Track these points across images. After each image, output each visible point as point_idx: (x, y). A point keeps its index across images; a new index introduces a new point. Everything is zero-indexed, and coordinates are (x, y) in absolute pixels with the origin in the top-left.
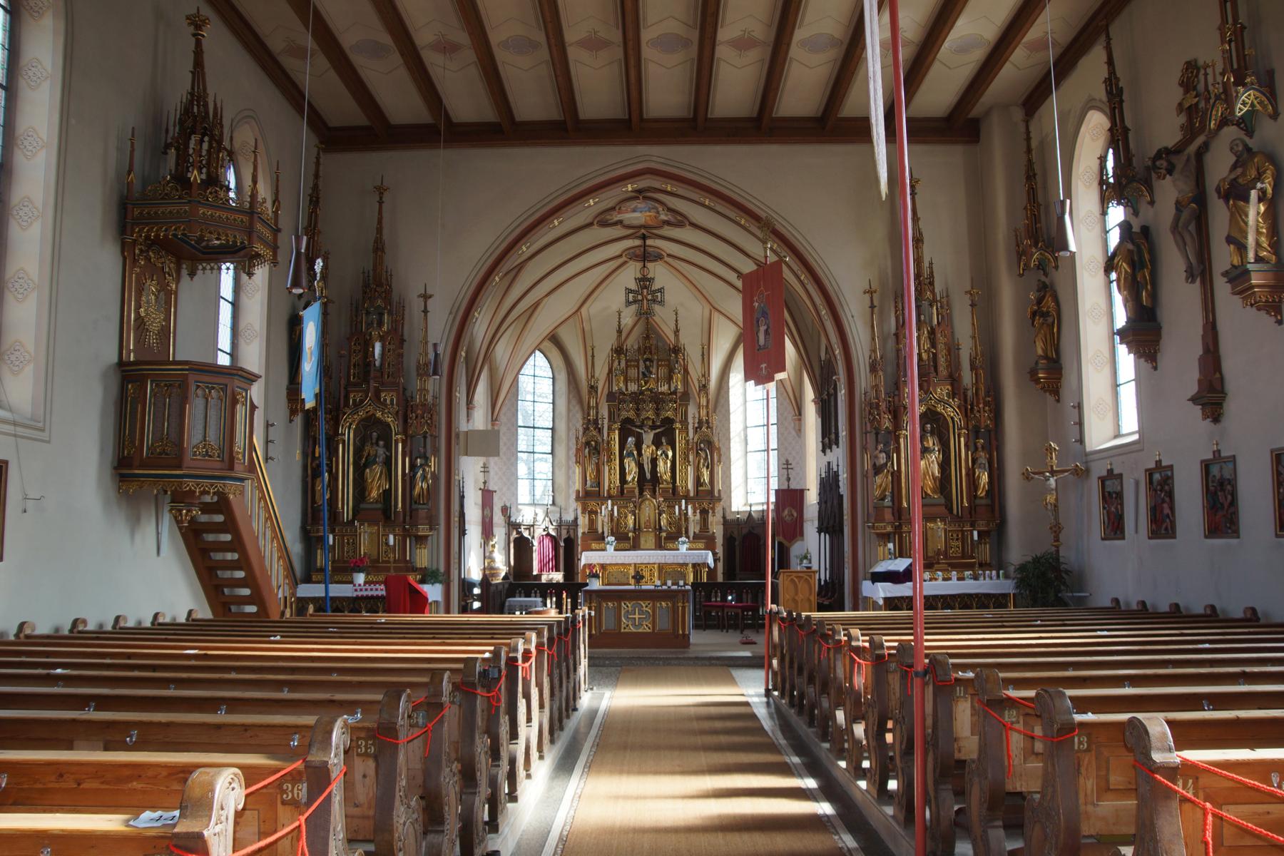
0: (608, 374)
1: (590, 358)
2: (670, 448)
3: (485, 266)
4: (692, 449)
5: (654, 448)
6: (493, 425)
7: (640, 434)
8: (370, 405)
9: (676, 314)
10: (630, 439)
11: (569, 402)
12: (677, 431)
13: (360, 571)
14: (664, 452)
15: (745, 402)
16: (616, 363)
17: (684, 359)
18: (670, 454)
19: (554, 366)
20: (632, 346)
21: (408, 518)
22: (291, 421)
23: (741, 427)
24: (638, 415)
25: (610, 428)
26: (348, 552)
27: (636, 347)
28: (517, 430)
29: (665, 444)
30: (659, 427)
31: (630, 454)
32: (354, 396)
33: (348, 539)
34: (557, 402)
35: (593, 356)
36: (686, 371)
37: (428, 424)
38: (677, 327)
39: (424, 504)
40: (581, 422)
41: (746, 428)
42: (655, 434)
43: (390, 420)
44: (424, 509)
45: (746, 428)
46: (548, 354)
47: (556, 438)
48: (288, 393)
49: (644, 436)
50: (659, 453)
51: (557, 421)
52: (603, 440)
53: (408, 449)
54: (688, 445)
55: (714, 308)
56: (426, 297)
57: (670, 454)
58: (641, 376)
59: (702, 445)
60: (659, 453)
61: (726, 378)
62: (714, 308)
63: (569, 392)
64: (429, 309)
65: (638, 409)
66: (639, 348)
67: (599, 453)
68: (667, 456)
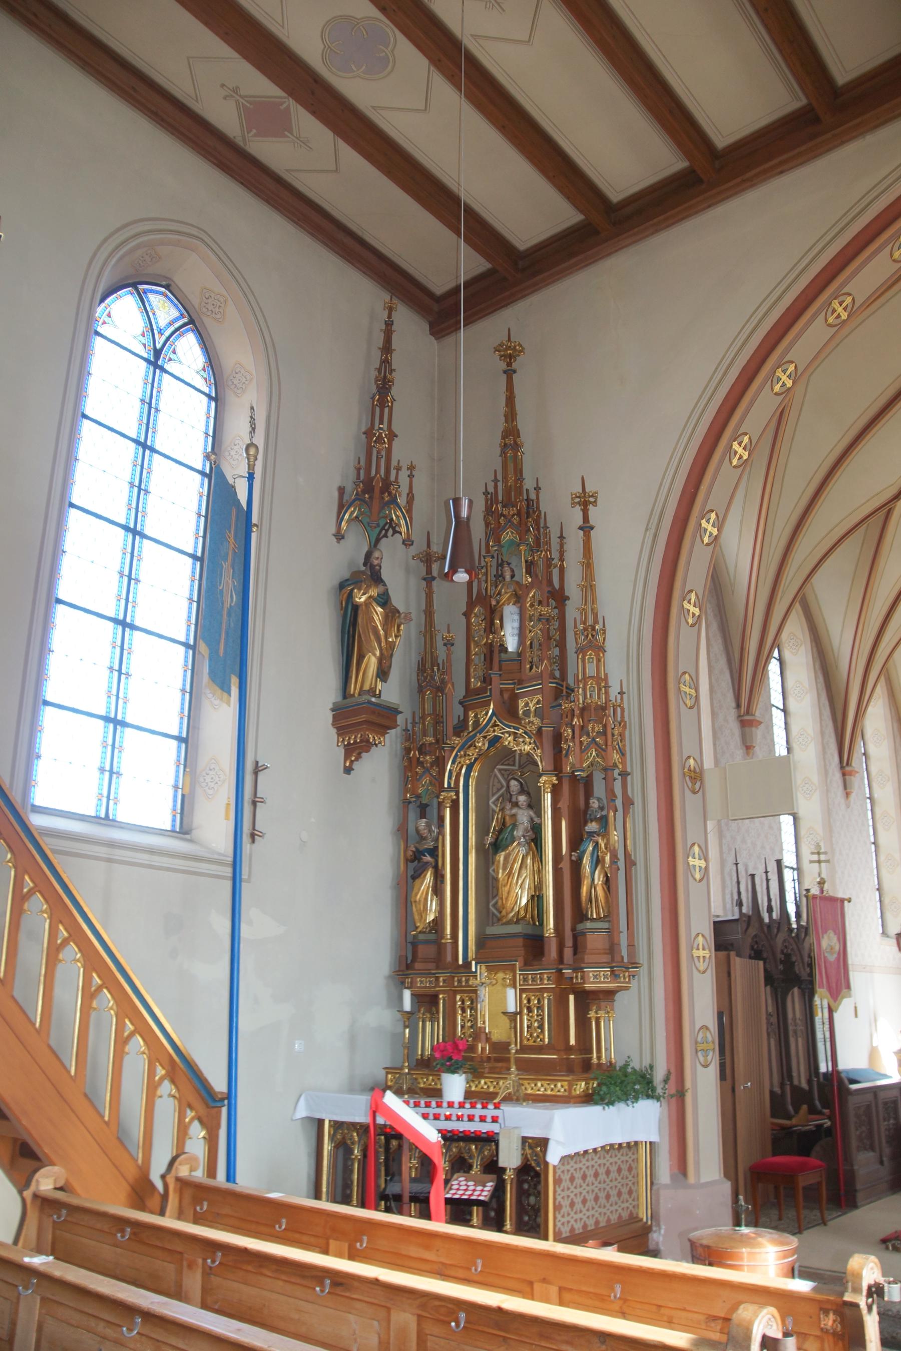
3: (702, 422)
8: (495, 725)
13: (453, 1069)
21: (568, 952)
22: (348, 770)
26: (462, 1027)
32: (476, 716)
33: (463, 1002)
37: (596, 743)
39: (599, 919)
43: (527, 748)
44: (595, 930)
48: (334, 717)
53: (564, 804)
56: (585, 501)
64: (592, 522)
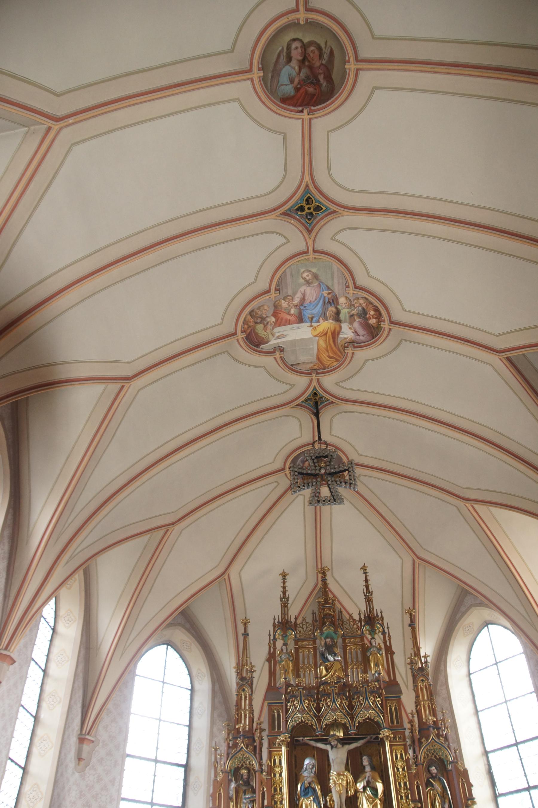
0: (269, 660)
1: (241, 638)
2: (377, 775)
4: (417, 776)
5: (350, 778)
6: (81, 740)
7: (325, 753)
9: (365, 573)
10: (307, 761)
11: (213, 722)
12: (387, 744)
14: (368, 782)
15: (477, 712)
16: (279, 643)
17: (384, 633)
18: (380, 787)
19: (194, 672)
20: (304, 619)
23: (480, 750)
24: (319, 721)
25: (271, 744)
27: (309, 620)
28: (123, 762)
29: (368, 769)
30: (355, 740)
31: (308, 790)
34: (195, 724)
35: (246, 635)
36: (389, 650)
38: (367, 587)
40: (224, 734)
41: (486, 753)
42: (350, 752)
45: (486, 753)
46: (185, 653)
47: (192, 779)
49: (332, 755)
50: (360, 786)
51: (193, 753)
52: (261, 765)
54: (409, 768)
55: (419, 558)
57: (380, 787)
58: (319, 661)
59: (433, 769)
60: (360, 786)
61: (441, 678)
62: (419, 558)
63: (214, 707)
65: (319, 709)
66: (314, 620)
67: (254, 791)
68: (375, 790)
